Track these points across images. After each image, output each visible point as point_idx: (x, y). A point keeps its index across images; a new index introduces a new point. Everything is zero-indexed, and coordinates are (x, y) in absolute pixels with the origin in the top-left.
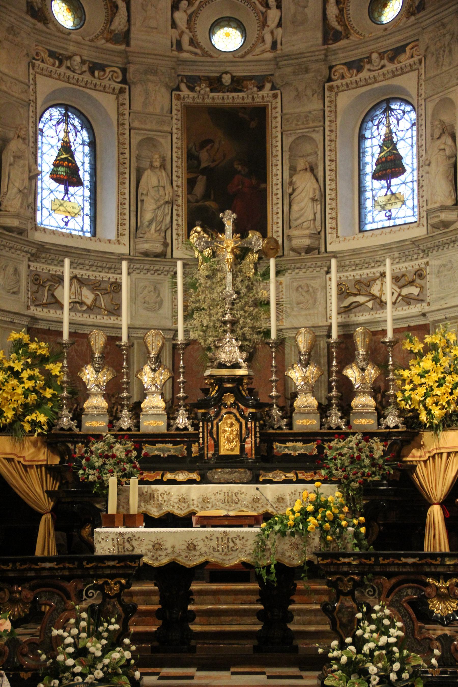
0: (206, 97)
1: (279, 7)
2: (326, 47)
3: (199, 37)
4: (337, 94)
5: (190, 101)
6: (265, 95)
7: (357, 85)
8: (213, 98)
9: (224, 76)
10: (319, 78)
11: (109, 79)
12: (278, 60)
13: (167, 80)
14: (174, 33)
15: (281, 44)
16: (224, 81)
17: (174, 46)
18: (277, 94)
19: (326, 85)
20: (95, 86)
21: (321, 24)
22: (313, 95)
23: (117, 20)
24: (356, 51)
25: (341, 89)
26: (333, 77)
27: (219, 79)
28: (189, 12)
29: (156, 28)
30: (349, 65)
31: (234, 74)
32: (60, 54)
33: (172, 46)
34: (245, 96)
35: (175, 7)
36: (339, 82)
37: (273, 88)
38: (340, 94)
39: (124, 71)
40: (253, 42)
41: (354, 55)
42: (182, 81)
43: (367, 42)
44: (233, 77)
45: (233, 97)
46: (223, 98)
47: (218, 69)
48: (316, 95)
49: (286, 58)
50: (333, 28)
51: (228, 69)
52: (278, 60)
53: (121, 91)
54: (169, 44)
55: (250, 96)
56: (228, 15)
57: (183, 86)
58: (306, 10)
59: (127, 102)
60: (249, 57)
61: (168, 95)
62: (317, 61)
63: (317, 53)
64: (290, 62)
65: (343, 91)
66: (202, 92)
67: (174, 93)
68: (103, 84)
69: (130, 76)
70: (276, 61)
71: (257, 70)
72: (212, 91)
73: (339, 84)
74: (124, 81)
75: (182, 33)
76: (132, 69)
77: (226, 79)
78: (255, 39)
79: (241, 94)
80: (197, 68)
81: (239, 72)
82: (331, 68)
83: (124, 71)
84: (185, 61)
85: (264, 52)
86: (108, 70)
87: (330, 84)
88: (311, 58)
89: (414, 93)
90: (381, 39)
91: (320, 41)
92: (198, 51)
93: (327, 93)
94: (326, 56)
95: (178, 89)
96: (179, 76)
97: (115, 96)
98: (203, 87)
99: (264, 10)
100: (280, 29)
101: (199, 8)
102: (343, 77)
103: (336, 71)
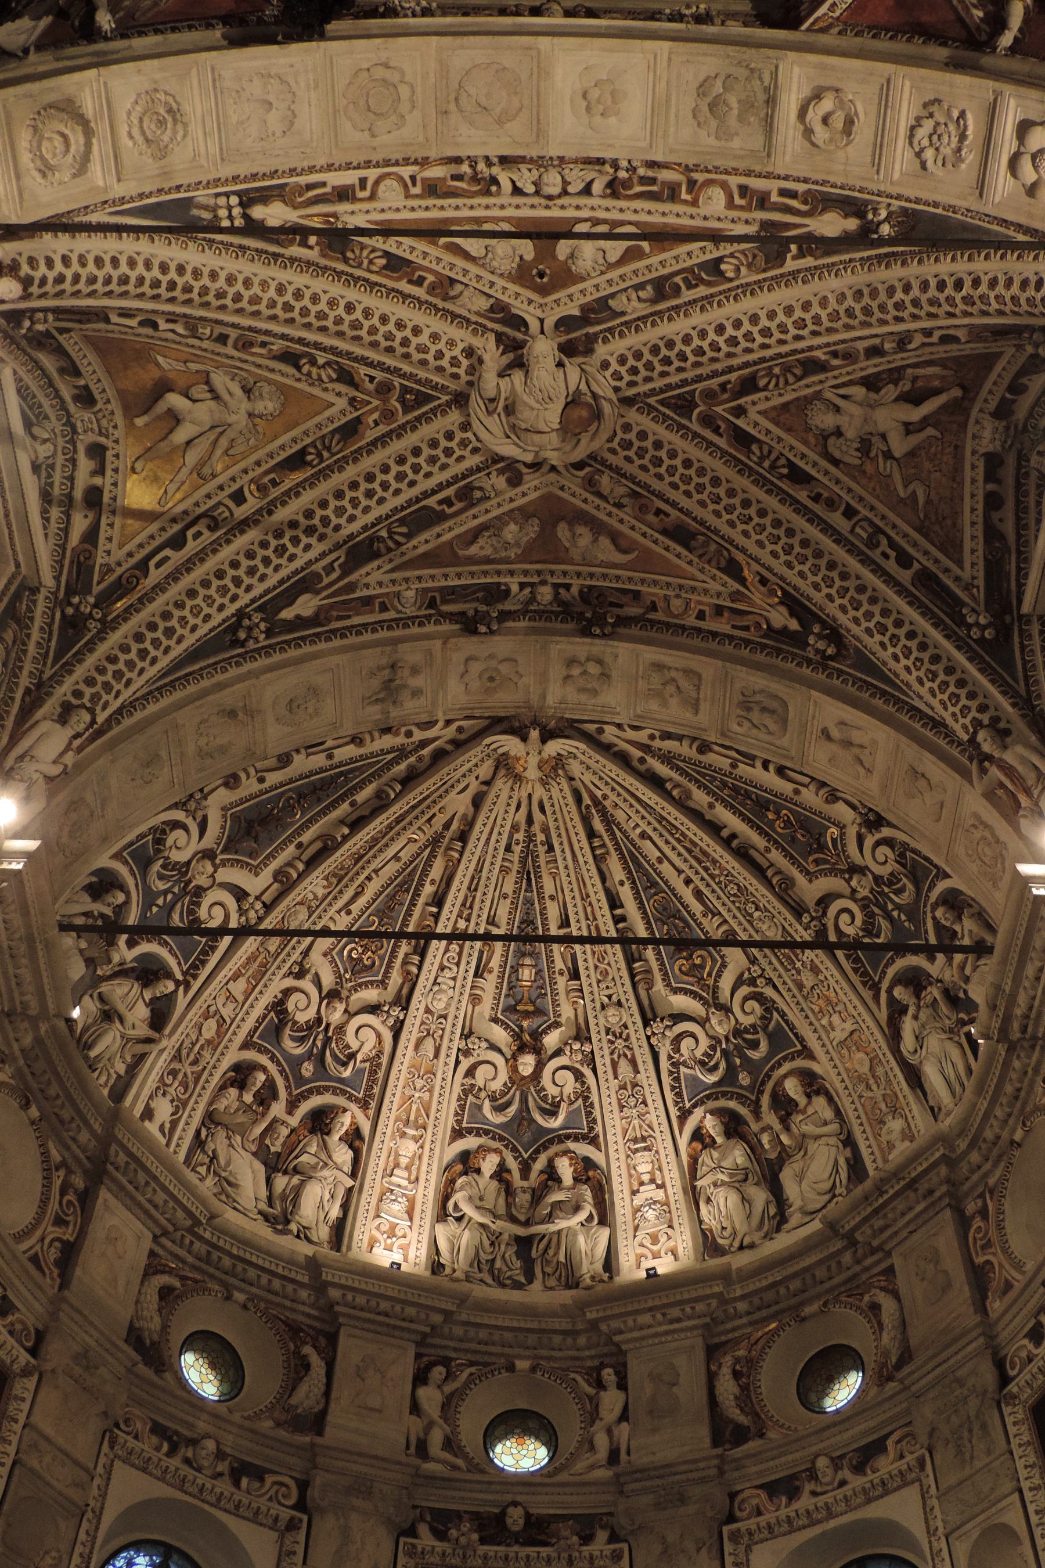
0: (469, 1553)
1: (622, 1386)
2: (719, 1451)
3: (462, 1437)
4: (748, 1549)
5: (436, 1559)
6: (596, 1553)
7: (791, 1526)
8: (485, 1557)
9: (510, 1510)
10: (710, 1514)
11: (270, 1499)
12: (622, 1480)
13: (391, 1510)
14: (415, 1425)
15: (628, 1453)
16: (509, 1521)
17: (412, 1450)
18: (622, 1551)
19: (725, 1529)
20: (237, 1507)
21: (706, 1412)
22: (698, 1550)
23: (302, 1390)
24: (783, 1459)
25: (756, 1537)
26: (738, 1514)
27: (500, 1519)
28: (448, 1389)
29: (380, 1411)
30: (772, 1489)
31: (531, 1511)
32: (176, 1433)
33: (408, 1448)
34: (554, 1555)
35: (420, 1378)
36: (751, 1524)
37: (613, 1538)
38: (755, 1548)
39: (303, 1486)
40: (572, 1450)
41: (778, 1468)
42: (422, 1519)
43: (803, 1437)
44: (528, 1516)
45: (528, 1557)
46: (507, 1558)
47: (498, 1497)
48: (704, 1550)
49: (638, 1475)
50: (732, 1421)
51: (519, 1498)
52: (622, 1480)
53: (292, 1526)
54: (403, 1441)
55: (564, 1555)
56: (524, 1406)
57: (423, 1529)
58: (675, 1389)
59: (300, 1550)
60: (563, 1477)
61: (388, 1545)
62: (703, 1480)
63: (702, 1465)
64: (648, 1483)
65: (762, 1541)
66: (463, 1540)
67: (402, 1540)
68: (254, 1505)
69: (314, 1493)
70: (618, 1485)
71: (580, 1504)
72: (483, 1541)
73: (754, 1527)
74: (301, 1505)
75: (430, 1425)
76: (319, 1479)
77: (515, 1518)
78: (575, 1444)
79: (545, 1551)
80: (455, 1493)
81: (542, 1506)
82: (732, 1496)
83: (303, 1486)
84: (431, 1478)
85: (592, 1467)
86: (269, 1479)
87: (734, 1526)
88: (691, 1476)
89: (919, 1532)
90: (833, 1430)
91: (707, 1442)
92: (460, 1462)
93: (728, 1547)
94: (721, 1473)
95: (411, 1532)
96: (415, 1507)
97: (275, 1535)
98: (464, 1529)
99: (591, 1391)
100: (624, 1424)
101: (467, 1385)
102: (759, 1513)
103: (743, 1501)
